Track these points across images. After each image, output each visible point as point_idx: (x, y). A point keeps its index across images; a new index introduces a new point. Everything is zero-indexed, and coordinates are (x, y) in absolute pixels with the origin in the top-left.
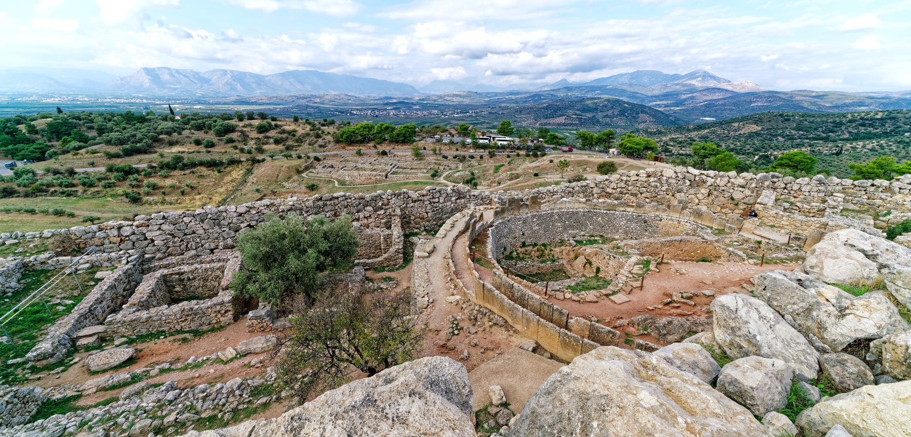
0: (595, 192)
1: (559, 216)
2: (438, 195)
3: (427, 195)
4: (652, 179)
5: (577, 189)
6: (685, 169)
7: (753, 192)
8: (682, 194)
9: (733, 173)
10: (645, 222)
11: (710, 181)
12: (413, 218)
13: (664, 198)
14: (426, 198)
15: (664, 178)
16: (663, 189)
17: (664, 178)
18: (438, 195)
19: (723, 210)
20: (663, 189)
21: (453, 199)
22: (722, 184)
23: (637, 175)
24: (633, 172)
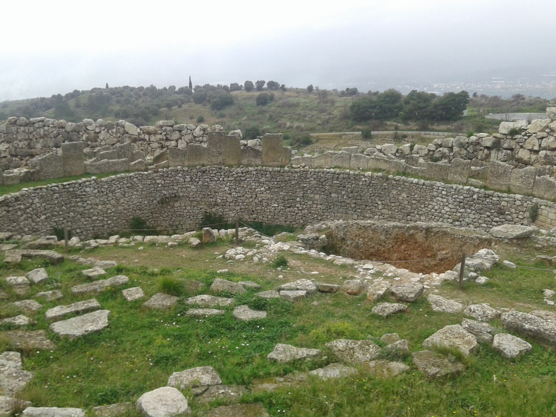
2: (176, 135)
3: (155, 133)
14: (153, 138)
18: (176, 135)
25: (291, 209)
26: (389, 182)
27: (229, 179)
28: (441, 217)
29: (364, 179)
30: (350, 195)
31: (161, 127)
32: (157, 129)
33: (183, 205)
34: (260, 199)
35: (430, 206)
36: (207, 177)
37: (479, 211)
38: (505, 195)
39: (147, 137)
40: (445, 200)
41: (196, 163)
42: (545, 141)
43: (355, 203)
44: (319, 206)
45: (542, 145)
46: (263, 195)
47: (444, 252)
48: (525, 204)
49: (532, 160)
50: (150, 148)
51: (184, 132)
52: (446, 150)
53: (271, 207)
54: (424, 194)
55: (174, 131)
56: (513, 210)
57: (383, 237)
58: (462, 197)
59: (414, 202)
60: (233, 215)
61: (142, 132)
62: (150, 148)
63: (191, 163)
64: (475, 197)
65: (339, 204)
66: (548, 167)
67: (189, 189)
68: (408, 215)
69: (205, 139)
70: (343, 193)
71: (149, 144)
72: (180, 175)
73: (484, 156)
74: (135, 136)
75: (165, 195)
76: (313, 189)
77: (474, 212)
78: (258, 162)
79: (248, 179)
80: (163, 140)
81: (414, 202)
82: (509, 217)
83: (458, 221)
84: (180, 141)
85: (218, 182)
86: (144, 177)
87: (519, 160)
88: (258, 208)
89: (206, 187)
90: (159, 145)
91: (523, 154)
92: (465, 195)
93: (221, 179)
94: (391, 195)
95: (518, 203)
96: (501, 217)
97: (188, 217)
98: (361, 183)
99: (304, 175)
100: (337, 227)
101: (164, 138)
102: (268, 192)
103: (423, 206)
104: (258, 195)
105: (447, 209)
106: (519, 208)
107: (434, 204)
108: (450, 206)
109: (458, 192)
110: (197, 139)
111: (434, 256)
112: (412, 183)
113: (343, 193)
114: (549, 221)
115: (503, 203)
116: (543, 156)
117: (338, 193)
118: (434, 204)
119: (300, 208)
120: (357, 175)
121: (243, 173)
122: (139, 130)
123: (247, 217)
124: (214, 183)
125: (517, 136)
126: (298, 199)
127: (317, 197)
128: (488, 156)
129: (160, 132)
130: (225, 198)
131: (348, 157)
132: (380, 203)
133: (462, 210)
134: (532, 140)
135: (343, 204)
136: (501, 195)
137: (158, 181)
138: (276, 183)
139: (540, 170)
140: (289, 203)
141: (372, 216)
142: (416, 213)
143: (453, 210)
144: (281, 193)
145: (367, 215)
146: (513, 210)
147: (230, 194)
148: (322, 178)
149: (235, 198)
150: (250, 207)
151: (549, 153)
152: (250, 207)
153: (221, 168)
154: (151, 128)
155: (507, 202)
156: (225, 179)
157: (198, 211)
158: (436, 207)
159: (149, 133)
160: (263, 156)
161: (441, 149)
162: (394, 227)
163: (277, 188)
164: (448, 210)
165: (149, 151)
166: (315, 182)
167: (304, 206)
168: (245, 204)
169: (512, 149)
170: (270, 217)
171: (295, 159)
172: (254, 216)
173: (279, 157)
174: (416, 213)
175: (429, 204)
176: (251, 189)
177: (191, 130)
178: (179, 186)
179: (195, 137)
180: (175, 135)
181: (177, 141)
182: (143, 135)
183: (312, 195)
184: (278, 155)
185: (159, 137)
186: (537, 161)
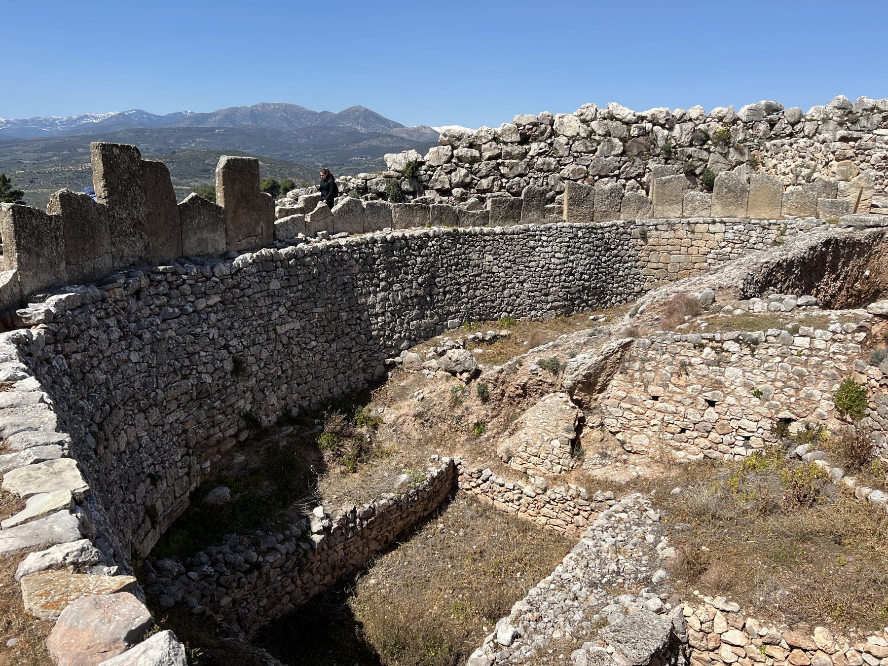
4: (534, 148)
15: (563, 140)
16: (566, 171)
23: (495, 139)
28: (551, 276)
35: (533, 264)
42: (456, 175)
58: (567, 239)
68: (504, 289)
77: (584, 256)
85: (184, 319)
95: (621, 230)
106: (624, 236)
107: (536, 258)
112: (495, 234)
115: (606, 235)
118: (536, 258)
133: (572, 258)
134: (440, 175)
138: (300, 287)
142: (515, 281)
144: (315, 310)
147: (226, 347)
150: (273, 369)
155: (610, 232)
156: (201, 304)
163: (305, 300)
172: (284, 387)
174: (515, 281)
175: (530, 261)
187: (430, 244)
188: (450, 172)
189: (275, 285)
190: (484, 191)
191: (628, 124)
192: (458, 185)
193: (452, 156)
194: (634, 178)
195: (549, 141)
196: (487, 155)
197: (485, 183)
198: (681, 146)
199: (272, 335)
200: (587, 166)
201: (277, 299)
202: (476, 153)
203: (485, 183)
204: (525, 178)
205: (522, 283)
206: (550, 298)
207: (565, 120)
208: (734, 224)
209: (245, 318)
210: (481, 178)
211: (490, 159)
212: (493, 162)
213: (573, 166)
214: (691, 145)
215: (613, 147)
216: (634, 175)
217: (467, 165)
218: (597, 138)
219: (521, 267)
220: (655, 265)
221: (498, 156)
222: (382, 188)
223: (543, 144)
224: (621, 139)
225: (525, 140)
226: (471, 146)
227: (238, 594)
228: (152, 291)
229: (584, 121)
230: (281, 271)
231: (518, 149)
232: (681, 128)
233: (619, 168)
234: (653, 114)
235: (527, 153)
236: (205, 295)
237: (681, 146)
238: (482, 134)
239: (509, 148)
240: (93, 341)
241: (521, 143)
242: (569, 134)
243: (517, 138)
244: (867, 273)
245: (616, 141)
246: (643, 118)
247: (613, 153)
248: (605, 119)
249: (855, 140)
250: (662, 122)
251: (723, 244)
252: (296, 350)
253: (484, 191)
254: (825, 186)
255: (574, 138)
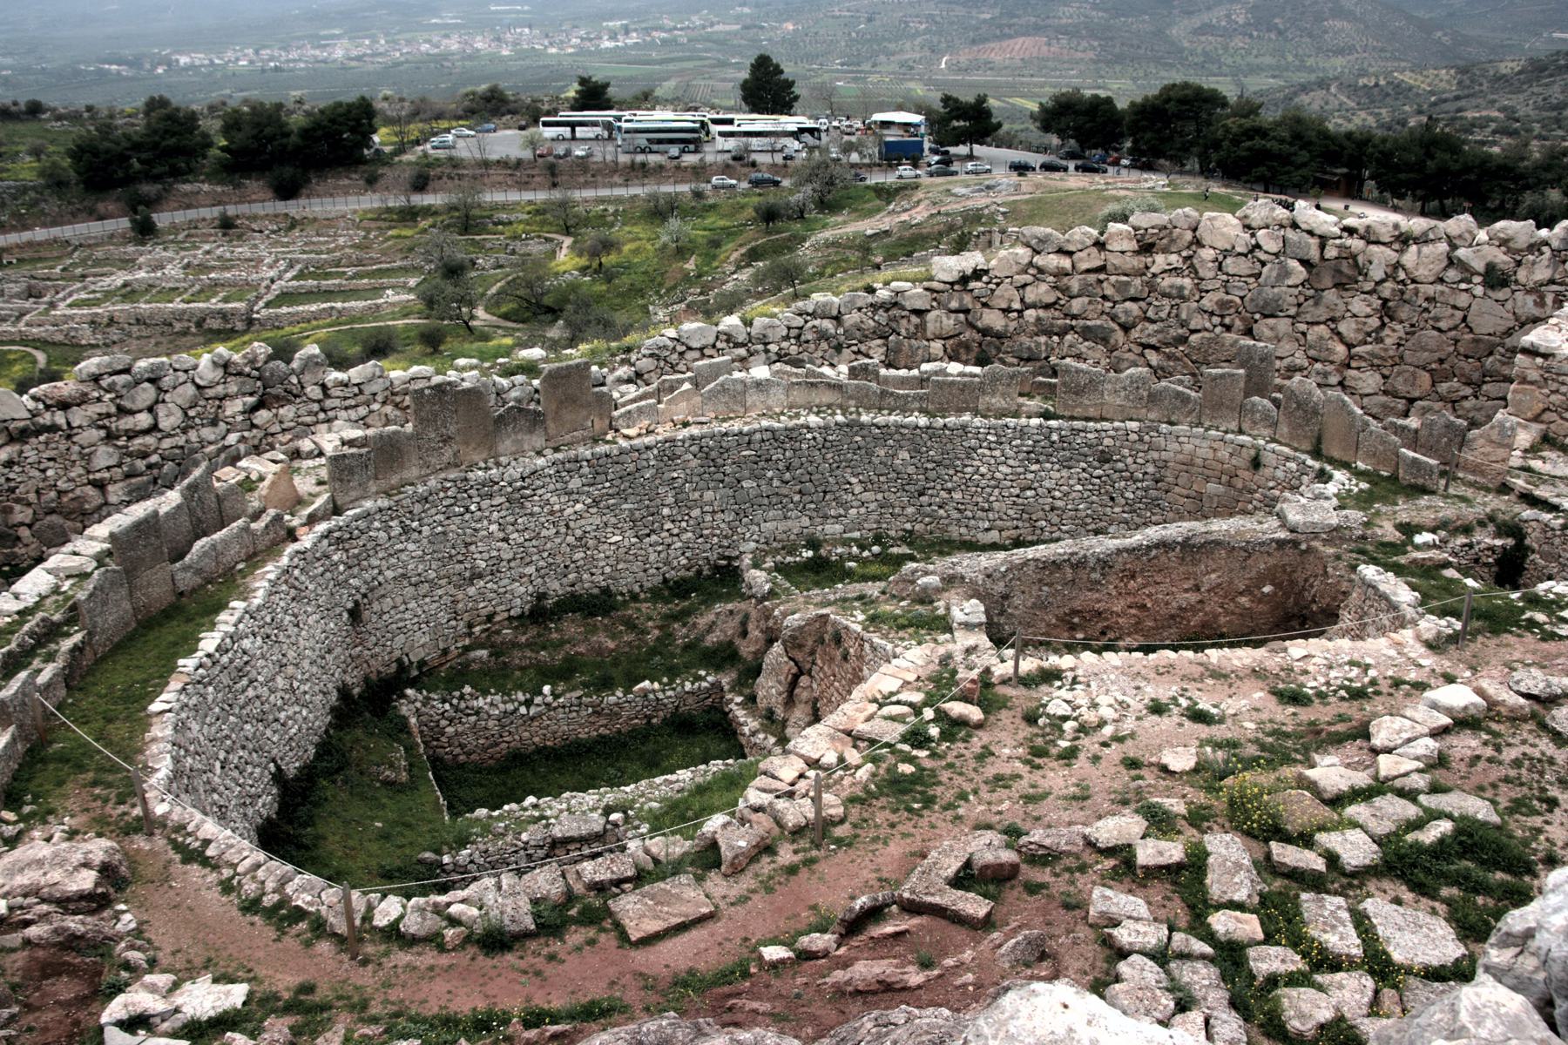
0: (931, 328)
1: (704, 454)
2: (147, 393)
3: (83, 400)
4: (1160, 261)
5: (851, 318)
6: (1281, 213)
7: (1541, 303)
8: (1283, 325)
9: (1462, 223)
10: (1104, 458)
11: (1381, 256)
12: (21, 514)
13: (1216, 340)
14: (78, 416)
16: (1208, 302)
17: (1207, 254)
18: (147, 393)
19: (1443, 387)
20: (1208, 302)
21: (234, 408)
22: (1422, 273)
23: (1100, 245)
24: (1083, 233)
25: (654, 538)
26: (865, 432)
27: (498, 500)
29: (809, 436)
30: (787, 476)
31: (96, 379)
32: (84, 388)
33: (399, 600)
34: (579, 533)
35: (969, 469)
36: (433, 511)
37: (1066, 464)
38: (1106, 425)
39: (60, 418)
40: (997, 453)
41: (395, 480)
43: (800, 492)
44: (719, 516)
45: (1027, 300)
46: (583, 522)
47: (1213, 576)
48: (1147, 438)
49: (1011, 329)
50: (76, 448)
51: (166, 382)
52: (827, 325)
53: (606, 546)
54: (949, 446)
55: (137, 383)
56: (1126, 452)
57: (1095, 576)
59: (930, 466)
60: (523, 589)
61: (41, 406)
62: (76, 448)
63: (383, 484)
64: (1055, 437)
65: (766, 501)
66: (1043, 339)
67: (403, 556)
68: (921, 494)
69: (233, 389)
70: (770, 474)
71: (69, 437)
72: (377, 524)
73: (912, 329)
74: (22, 424)
75: (357, 589)
76: (696, 479)
78: (538, 441)
79: (539, 492)
80: (109, 415)
81: (930, 466)
82: (1120, 465)
83: (1030, 488)
84: (161, 410)
85: (467, 516)
86: (309, 556)
87: (985, 332)
88: (576, 557)
89: (442, 538)
90: (102, 433)
91: (993, 319)
92: (1036, 437)
93: (473, 508)
94: (876, 460)
95: (1133, 437)
96: (1106, 466)
97: (416, 627)
98: (804, 446)
99: (669, 453)
100: (989, 576)
101: (113, 410)
102: (594, 510)
103: (951, 472)
104: (572, 524)
105: (1003, 468)
108: (1011, 462)
109: (1022, 433)
110: (210, 393)
111: (1197, 588)
112: (917, 427)
113: (770, 474)
114: (1199, 461)
116: (1032, 320)
117: (757, 478)
119: (676, 531)
120: (793, 429)
121: (523, 479)
122: (31, 405)
123: (555, 585)
124: (457, 520)
125: (972, 285)
126: (666, 511)
127: (709, 495)
128: (922, 327)
129: (96, 394)
130: (494, 553)
131: (739, 387)
132: (854, 480)
133: (1034, 467)
135: (774, 500)
136: (1098, 426)
137: (335, 558)
139: (1029, 348)
140: (644, 524)
141: (842, 512)
143: (1021, 470)
145: (833, 512)
146: (1126, 452)
147: (505, 540)
148: (711, 449)
149: (520, 545)
150: (559, 559)
151: (1041, 313)
152: (559, 559)
153: (466, 479)
154: (66, 387)
156: (485, 504)
157: (435, 605)
158: (983, 470)
159: (64, 406)
160: (551, 425)
161: (817, 322)
162: (1119, 551)
164: (1009, 470)
165: (74, 457)
166: (695, 463)
167: (684, 524)
168: (545, 554)
169: (967, 311)
170: (608, 570)
171: (621, 416)
172: (572, 576)
173: (587, 418)
176: (552, 513)
177: (186, 371)
178: (380, 555)
179: (199, 387)
180: (145, 396)
181: (150, 409)
182: (48, 415)
183: (697, 495)
184: (585, 413)
185: (93, 410)
186: (1019, 331)
187: (809, 436)
188: (1024, 286)
189: (575, 483)
190: (1074, 317)
191: (1323, 240)
192: (1034, 306)
193: (1030, 264)
194: (1324, 323)
195: (1184, 254)
196: (1084, 266)
197: (1077, 305)
198: (1414, 281)
199: (563, 530)
200: (1242, 298)
201: (575, 497)
202: (1066, 263)
203: (1077, 305)
204: (1142, 304)
205: (949, 491)
206: (991, 515)
207: (1217, 224)
208: (1288, 459)
209: (532, 514)
210: (1072, 297)
211: (1088, 271)
212: (1092, 278)
213: (1221, 295)
214: (1441, 280)
215: (1285, 273)
216: (1322, 319)
217: (1051, 279)
218: (1263, 257)
219: (951, 472)
220: (1185, 492)
221: (1102, 269)
222: (919, 305)
223: (1173, 258)
224: (1305, 263)
225: (1146, 248)
226: (1061, 251)
227: (460, 728)
228: (442, 495)
229: (1247, 227)
230: (586, 470)
231: (1137, 262)
232: (1419, 252)
233: (1299, 305)
234: (1368, 227)
235: (1147, 268)
236: (491, 496)
237: (1414, 281)
238: (1077, 237)
239: (1115, 260)
240: (374, 539)
241: (1137, 253)
242: (1222, 244)
243: (1134, 245)
244: (1267, 589)
245: (1294, 264)
246: (1350, 231)
247: (1290, 282)
248: (1282, 226)
249: (1545, 356)
250: (1387, 240)
251: (1271, 484)
252: (591, 543)
253: (1074, 317)
254: (1447, 427)
255: (1226, 253)
